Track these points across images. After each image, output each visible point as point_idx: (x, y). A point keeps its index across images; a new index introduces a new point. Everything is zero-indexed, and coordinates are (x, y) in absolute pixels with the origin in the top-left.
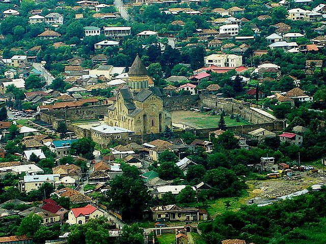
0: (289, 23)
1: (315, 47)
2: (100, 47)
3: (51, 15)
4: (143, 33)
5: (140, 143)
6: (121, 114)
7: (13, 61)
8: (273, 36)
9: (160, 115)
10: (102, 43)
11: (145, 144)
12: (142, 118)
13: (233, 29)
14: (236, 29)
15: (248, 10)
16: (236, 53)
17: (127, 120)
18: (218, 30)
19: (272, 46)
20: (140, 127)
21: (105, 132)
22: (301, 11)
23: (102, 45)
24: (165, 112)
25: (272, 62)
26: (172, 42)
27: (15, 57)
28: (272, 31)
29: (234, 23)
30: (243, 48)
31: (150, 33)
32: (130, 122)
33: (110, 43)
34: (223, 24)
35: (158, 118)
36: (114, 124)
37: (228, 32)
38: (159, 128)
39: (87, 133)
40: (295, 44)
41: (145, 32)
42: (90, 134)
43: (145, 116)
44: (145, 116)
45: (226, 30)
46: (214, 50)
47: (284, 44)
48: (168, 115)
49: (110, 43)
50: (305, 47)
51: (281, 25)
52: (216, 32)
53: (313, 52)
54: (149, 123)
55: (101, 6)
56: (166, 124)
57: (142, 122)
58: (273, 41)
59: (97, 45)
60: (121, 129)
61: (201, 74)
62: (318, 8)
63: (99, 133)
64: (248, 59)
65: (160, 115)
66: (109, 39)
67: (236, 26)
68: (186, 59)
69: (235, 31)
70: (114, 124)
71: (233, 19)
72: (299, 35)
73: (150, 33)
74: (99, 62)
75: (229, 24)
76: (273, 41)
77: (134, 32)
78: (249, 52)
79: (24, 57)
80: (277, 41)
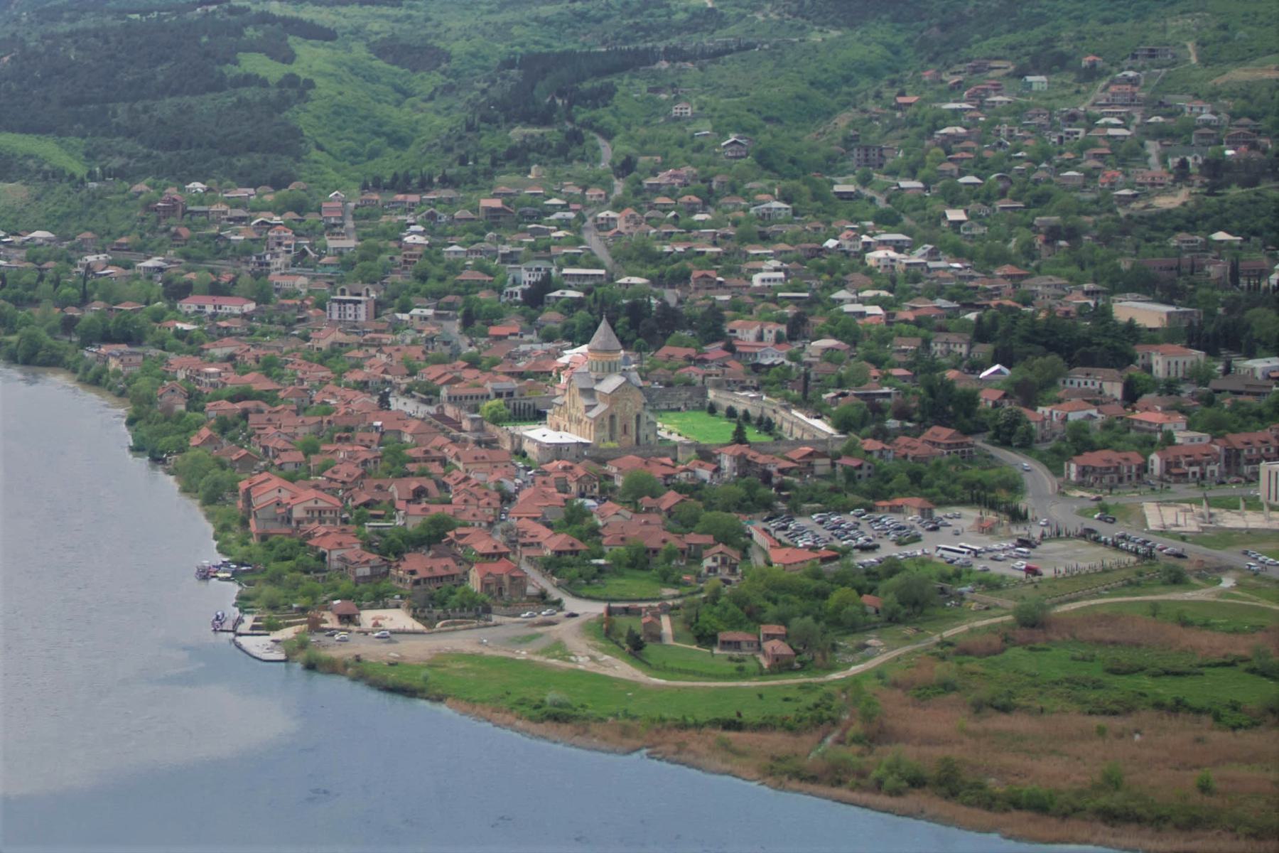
0: (870, 272)
1: (910, 316)
2: (553, 300)
4: (624, 280)
6: (573, 411)
9: (638, 417)
10: (557, 293)
12: (607, 422)
13: (775, 280)
14: (781, 280)
18: (750, 280)
20: (602, 434)
22: (892, 254)
23: (557, 298)
24: (647, 413)
28: (841, 285)
29: (777, 270)
30: (789, 311)
31: (636, 280)
32: (588, 426)
34: (760, 270)
37: (766, 284)
38: (634, 438)
39: (516, 441)
40: (877, 310)
42: (520, 444)
43: (612, 417)
44: (612, 417)
45: (763, 280)
47: (858, 308)
48: (652, 418)
49: (571, 294)
50: (893, 315)
51: (857, 277)
52: (745, 283)
53: (906, 322)
54: (619, 429)
55: (560, 234)
56: (647, 432)
57: (607, 428)
59: (549, 298)
61: (715, 350)
62: (920, 251)
63: (534, 441)
64: (796, 329)
65: (638, 417)
66: (570, 287)
67: (781, 275)
71: (775, 263)
72: (884, 293)
73: (636, 280)
76: (841, 301)
77: (611, 279)
80: (848, 301)
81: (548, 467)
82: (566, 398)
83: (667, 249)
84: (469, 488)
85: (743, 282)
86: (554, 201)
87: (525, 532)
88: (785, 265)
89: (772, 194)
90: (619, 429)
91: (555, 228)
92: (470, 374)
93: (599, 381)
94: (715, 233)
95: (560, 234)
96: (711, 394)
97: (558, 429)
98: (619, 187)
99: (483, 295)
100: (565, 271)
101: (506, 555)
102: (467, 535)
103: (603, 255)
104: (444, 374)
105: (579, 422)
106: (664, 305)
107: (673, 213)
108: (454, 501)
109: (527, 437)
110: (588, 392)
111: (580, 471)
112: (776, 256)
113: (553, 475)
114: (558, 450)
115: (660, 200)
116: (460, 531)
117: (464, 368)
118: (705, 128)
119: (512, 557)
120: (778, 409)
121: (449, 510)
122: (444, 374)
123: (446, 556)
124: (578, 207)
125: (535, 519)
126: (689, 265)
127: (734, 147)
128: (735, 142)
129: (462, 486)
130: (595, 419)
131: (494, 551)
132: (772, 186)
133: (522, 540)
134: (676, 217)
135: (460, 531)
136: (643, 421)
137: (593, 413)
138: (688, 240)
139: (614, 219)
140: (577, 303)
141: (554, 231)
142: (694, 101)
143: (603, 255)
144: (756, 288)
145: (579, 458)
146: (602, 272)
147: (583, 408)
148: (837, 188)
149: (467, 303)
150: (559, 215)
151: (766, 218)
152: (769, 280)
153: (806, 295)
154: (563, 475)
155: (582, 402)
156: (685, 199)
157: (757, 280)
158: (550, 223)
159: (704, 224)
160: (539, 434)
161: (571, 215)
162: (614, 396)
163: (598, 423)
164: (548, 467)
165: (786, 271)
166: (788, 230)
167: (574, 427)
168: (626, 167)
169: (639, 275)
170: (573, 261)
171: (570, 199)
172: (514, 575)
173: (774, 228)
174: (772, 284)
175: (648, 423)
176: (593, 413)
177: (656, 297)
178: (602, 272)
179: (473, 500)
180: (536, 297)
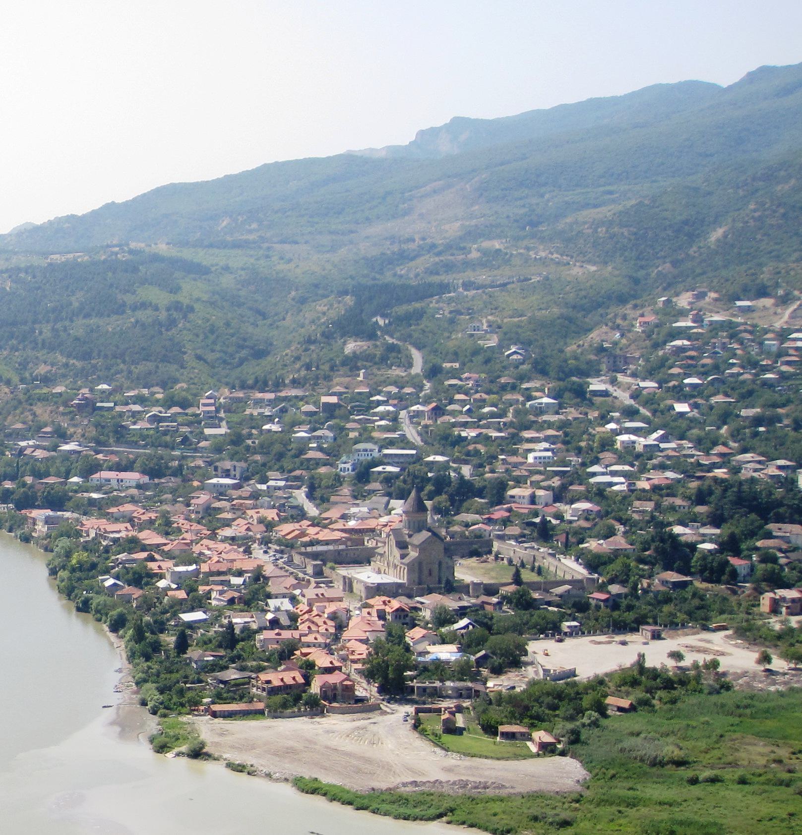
0: (615, 452)
3: (319, 433)
4: (431, 459)
5: (410, 596)
6: (391, 559)
7: (268, 487)
8: (595, 468)
9: (440, 564)
10: (379, 469)
11: (418, 599)
12: (416, 565)
13: (544, 458)
14: (549, 457)
15: (566, 434)
16: (545, 488)
17: (398, 568)
19: (592, 480)
21: (370, 581)
23: (379, 473)
25: (588, 499)
26: (466, 471)
27: (271, 483)
29: (546, 450)
30: (556, 482)
33: (389, 469)
35: (437, 566)
36: (382, 572)
41: (434, 456)
43: (420, 564)
45: (535, 458)
46: (519, 482)
49: (389, 469)
55: (383, 423)
58: (594, 474)
60: (390, 578)
63: (362, 582)
65: (440, 564)
66: (388, 464)
67: (549, 454)
68: (480, 493)
69: (547, 460)
70: (382, 572)
71: (546, 445)
74: (373, 492)
75: (540, 451)
76: (594, 474)
78: (564, 488)
79: (282, 483)
81: (371, 601)
82: (386, 549)
83: (464, 434)
84: (311, 618)
85: (520, 459)
86: (378, 398)
87: (353, 651)
88: (553, 446)
89: (543, 391)
90: (426, 572)
91: (378, 418)
92: (312, 531)
93: (410, 536)
94: (499, 423)
95: (383, 423)
96: (496, 546)
97: (379, 572)
98: (428, 385)
99: (322, 470)
100: (386, 451)
101: (340, 669)
102: (310, 653)
103: (416, 439)
104: (293, 531)
105: (395, 566)
106: (462, 477)
107: (468, 407)
108: (300, 628)
109: (356, 579)
110: (402, 545)
111: (395, 604)
112: (547, 439)
113: (376, 608)
114: (378, 590)
115: (458, 397)
116: (305, 650)
117: (308, 526)
118: (493, 342)
119: (344, 669)
120: (546, 556)
121: (296, 634)
122: (293, 531)
123: (293, 670)
124: (396, 402)
125: (361, 641)
126: (479, 446)
127: (515, 357)
128: (515, 353)
129: (306, 616)
130: (408, 565)
131: (331, 665)
132: (543, 385)
133: (351, 657)
134: (469, 410)
135: (305, 650)
136: (444, 565)
137: (407, 560)
138: (478, 427)
139: (422, 411)
140: (397, 476)
141: (377, 421)
142: (484, 321)
143: (416, 439)
144: (530, 464)
145: (395, 595)
146: (414, 452)
147: (398, 556)
148: (592, 388)
149: (312, 478)
150: (381, 409)
151: (540, 411)
152: (540, 458)
153: (568, 469)
154: (383, 607)
155: (397, 553)
156: (477, 396)
157: (531, 458)
158: (375, 414)
159: (492, 415)
160: (366, 575)
161: (391, 408)
162: (423, 548)
163: (411, 567)
164: (371, 602)
165: (552, 450)
166: (555, 418)
167: (391, 570)
168: (433, 372)
169: (442, 454)
170: (391, 443)
171: (389, 395)
172: (345, 683)
173: (545, 418)
174: (542, 460)
175: (448, 568)
176: (407, 560)
177: (455, 470)
178: (414, 452)
179: (314, 628)
180: (363, 474)
